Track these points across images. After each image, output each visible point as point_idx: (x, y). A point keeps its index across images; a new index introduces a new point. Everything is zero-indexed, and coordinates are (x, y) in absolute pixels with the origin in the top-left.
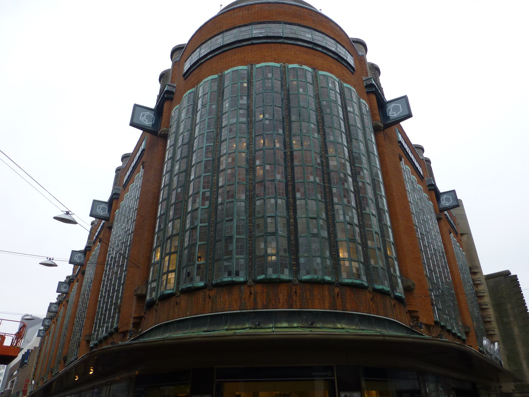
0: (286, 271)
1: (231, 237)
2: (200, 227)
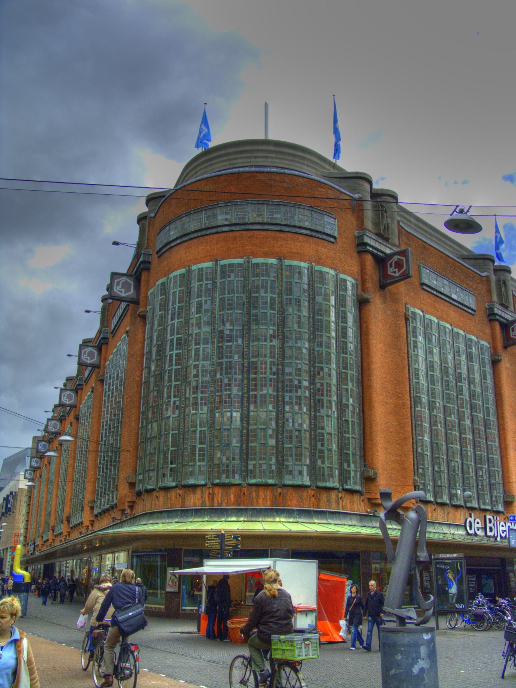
0: (237, 476)
1: (194, 447)
2: (172, 434)
